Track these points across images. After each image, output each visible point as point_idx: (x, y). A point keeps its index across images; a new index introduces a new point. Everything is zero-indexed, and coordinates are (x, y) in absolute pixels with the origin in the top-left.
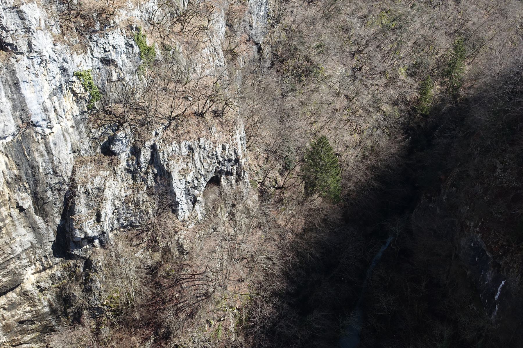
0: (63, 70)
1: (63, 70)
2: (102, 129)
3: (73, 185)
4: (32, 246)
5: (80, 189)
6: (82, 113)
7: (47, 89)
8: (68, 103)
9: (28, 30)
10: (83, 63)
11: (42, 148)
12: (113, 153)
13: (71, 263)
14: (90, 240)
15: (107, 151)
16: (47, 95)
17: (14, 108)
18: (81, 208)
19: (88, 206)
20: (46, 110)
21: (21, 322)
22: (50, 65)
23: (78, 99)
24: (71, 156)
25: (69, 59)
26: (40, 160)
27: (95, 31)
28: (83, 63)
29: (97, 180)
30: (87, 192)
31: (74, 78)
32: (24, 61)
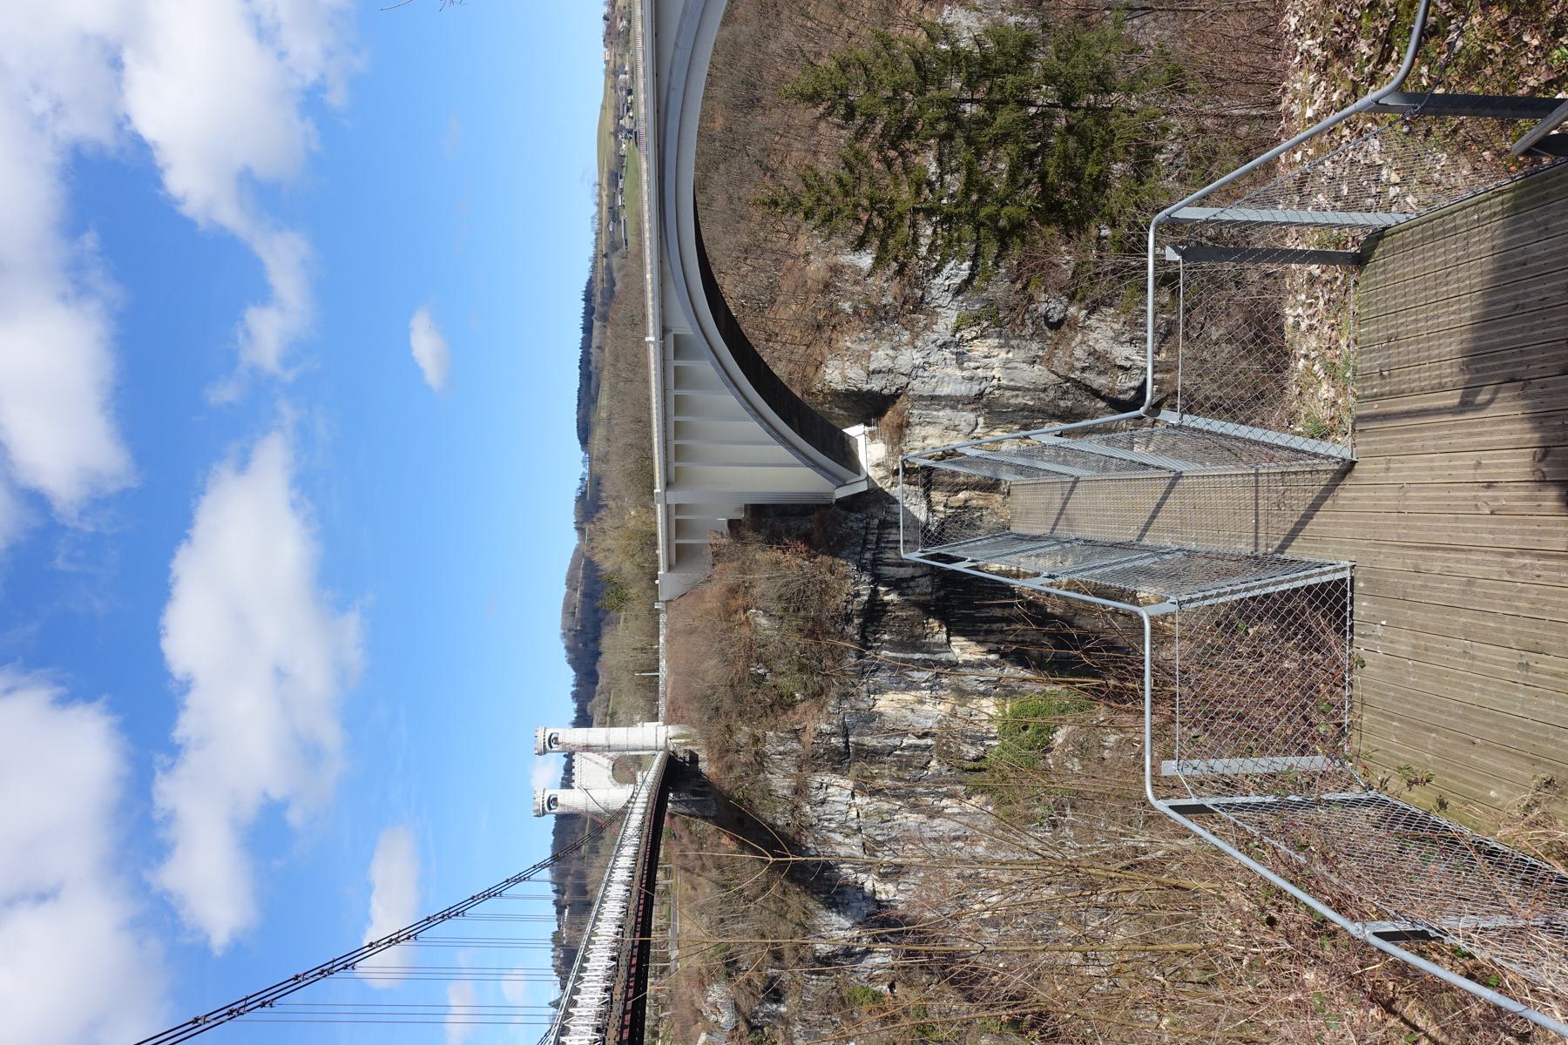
0: (944, 345)
1: (944, 345)
2: (1029, 322)
3: (1068, 380)
5: (1076, 375)
6: (1000, 336)
8: (980, 349)
9: (890, 371)
10: (948, 318)
11: (1008, 394)
12: (1061, 322)
15: (1056, 326)
16: (959, 373)
17: (953, 408)
18: (1098, 382)
19: (1100, 373)
20: (971, 379)
22: (931, 360)
23: (982, 336)
25: (935, 336)
26: (1020, 400)
27: (922, 298)
28: (948, 318)
29: (1079, 353)
30: (1083, 370)
32: (916, 384)
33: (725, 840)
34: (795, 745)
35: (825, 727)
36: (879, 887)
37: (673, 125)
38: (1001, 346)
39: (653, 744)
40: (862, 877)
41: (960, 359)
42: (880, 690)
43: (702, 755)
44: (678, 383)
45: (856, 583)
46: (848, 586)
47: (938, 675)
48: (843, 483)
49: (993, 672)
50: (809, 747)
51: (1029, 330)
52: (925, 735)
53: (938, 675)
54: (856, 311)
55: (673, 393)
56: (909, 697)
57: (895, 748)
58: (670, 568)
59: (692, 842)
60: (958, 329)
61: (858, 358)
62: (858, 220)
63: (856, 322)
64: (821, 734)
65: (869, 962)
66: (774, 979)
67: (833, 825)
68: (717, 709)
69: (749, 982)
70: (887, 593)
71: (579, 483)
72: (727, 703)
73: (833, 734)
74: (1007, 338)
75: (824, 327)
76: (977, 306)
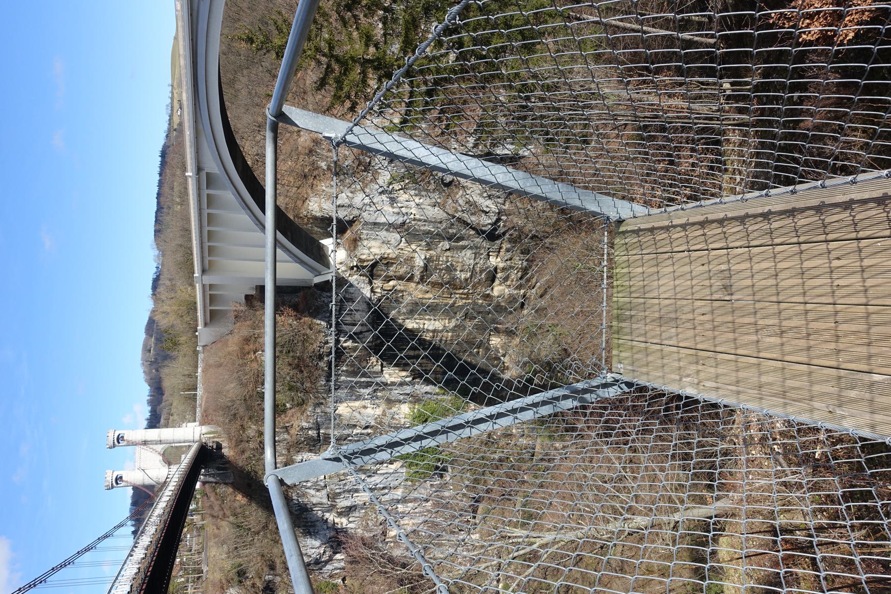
2: (432, 182)
4: (475, 254)
7: (388, 209)
8: (403, 197)
9: (349, 206)
10: (384, 177)
13: (507, 236)
14: (499, 220)
16: (391, 210)
20: (398, 214)
21: (521, 278)
24: (437, 208)
26: (426, 228)
27: (370, 163)
28: (384, 177)
31: (391, 187)
33: (239, 497)
34: (286, 436)
35: (305, 425)
36: (337, 520)
37: (202, 26)
38: (416, 195)
39: (191, 438)
40: (327, 515)
41: (393, 201)
42: (339, 401)
43: (224, 445)
44: (209, 205)
45: (326, 336)
46: (321, 337)
47: (375, 391)
48: (319, 274)
49: (408, 389)
50: (294, 437)
51: (432, 187)
52: (367, 427)
53: (375, 391)
54: (329, 168)
55: (206, 211)
56: (357, 404)
57: (349, 435)
58: (206, 325)
59: (217, 500)
60: (390, 184)
61: (329, 197)
62: (319, 63)
63: (329, 174)
64: (302, 429)
65: (329, 567)
66: (270, 581)
67: (309, 484)
68: (235, 415)
69: (253, 585)
70: (345, 341)
71: (155, 270)
72: (242, 411)
73: (310, 429)
74: (420, 191)
75: (308, 177)
76: (403, 170)
